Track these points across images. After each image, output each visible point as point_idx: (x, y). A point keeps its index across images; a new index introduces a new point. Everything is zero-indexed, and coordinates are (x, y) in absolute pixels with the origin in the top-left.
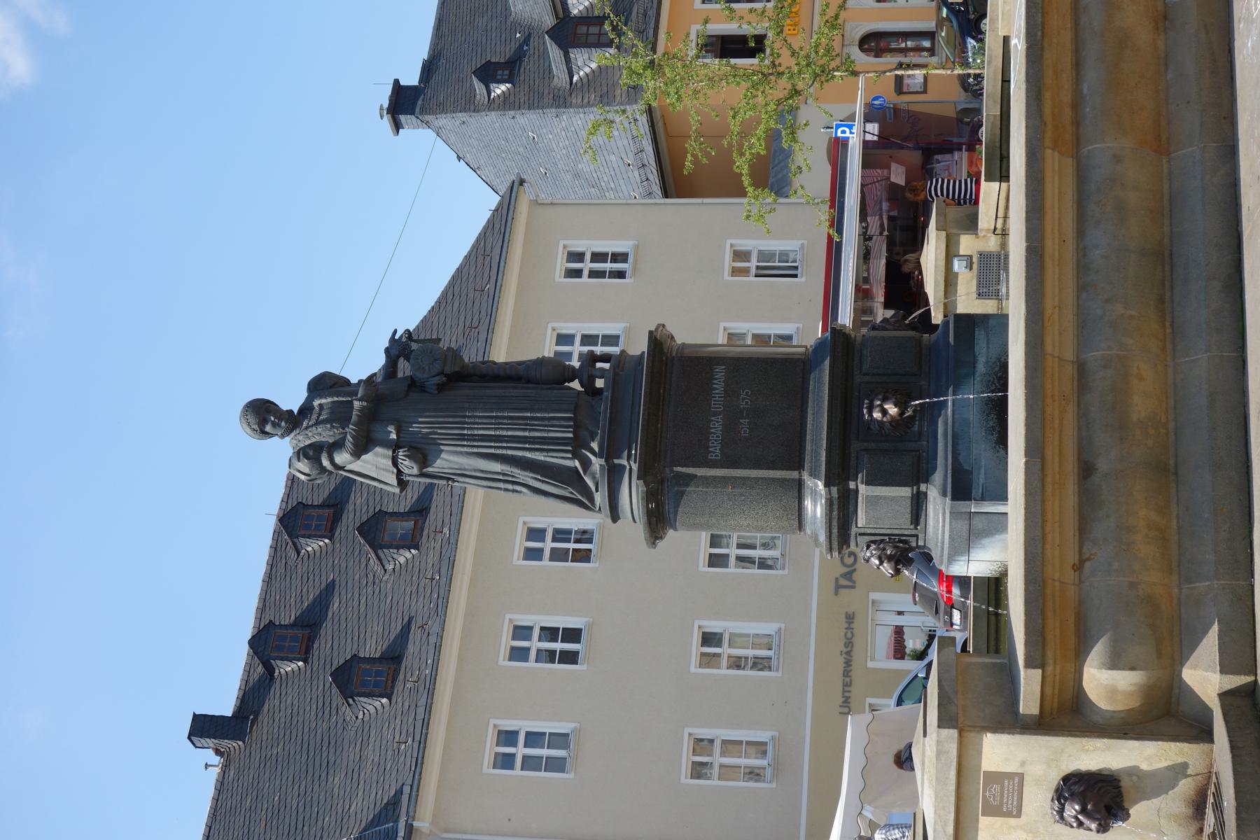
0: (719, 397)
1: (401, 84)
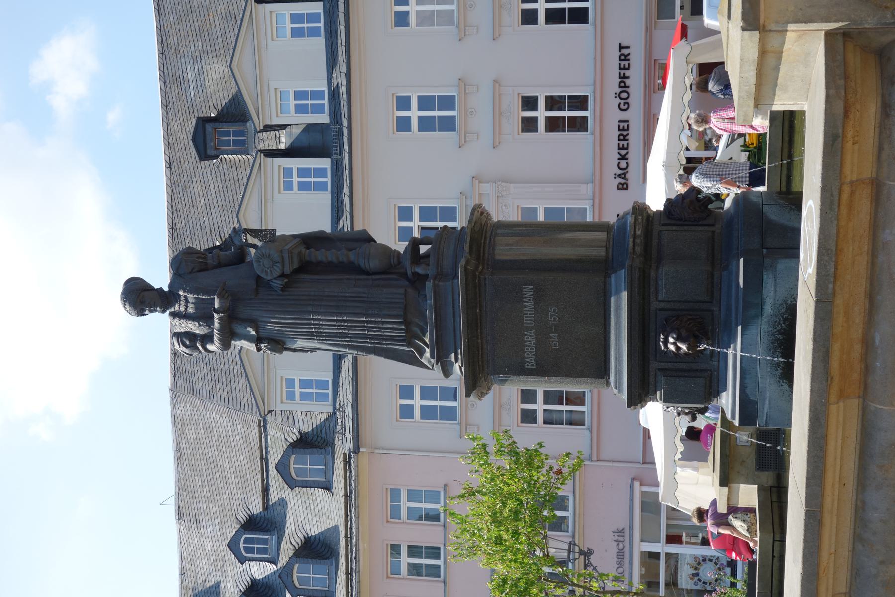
0: (529, 314)
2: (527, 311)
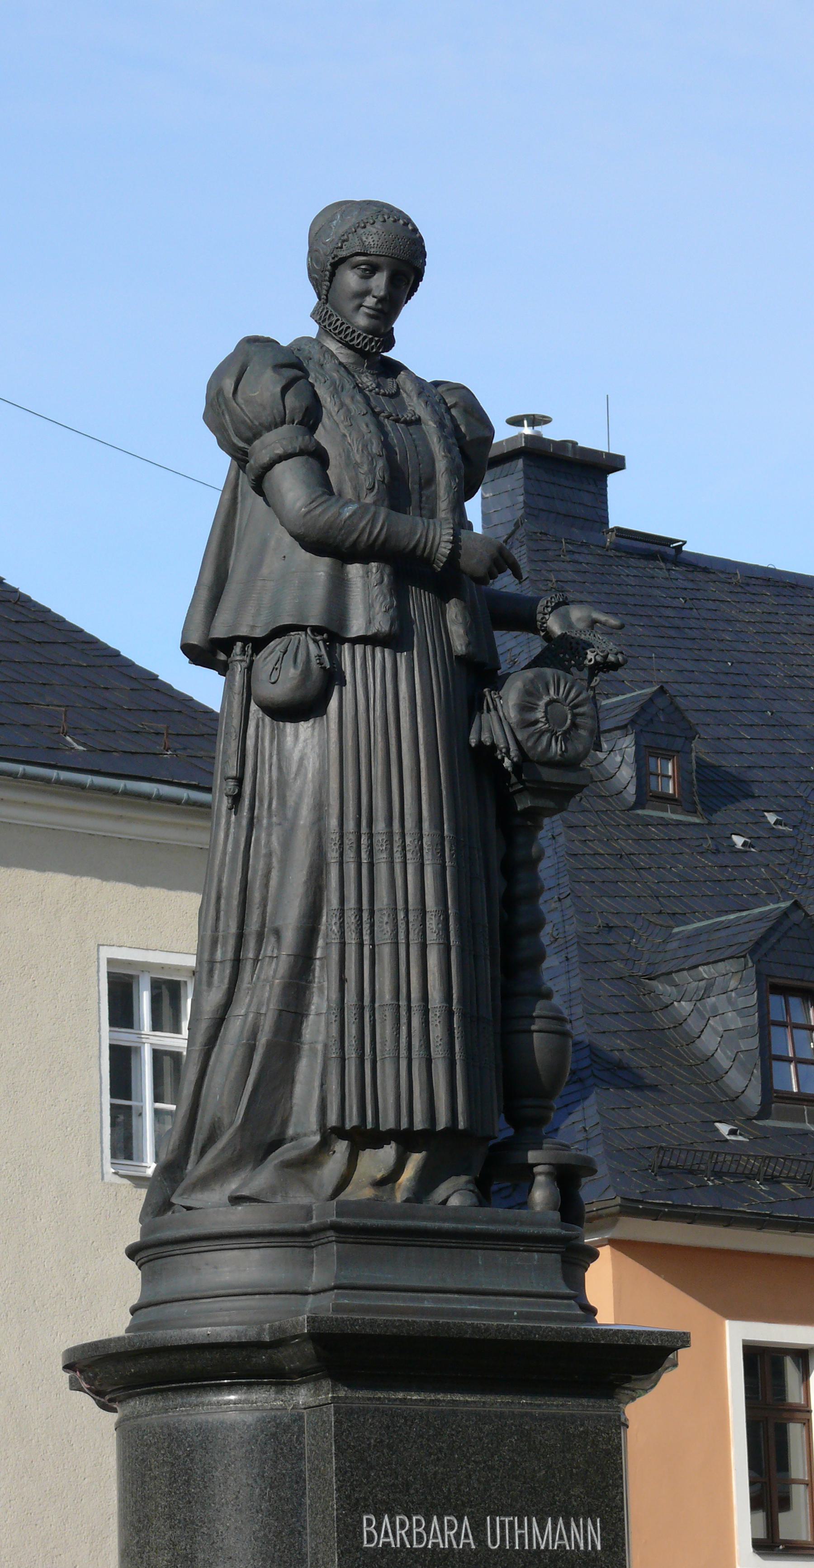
0: (521, 1536)
1: (613, 479)
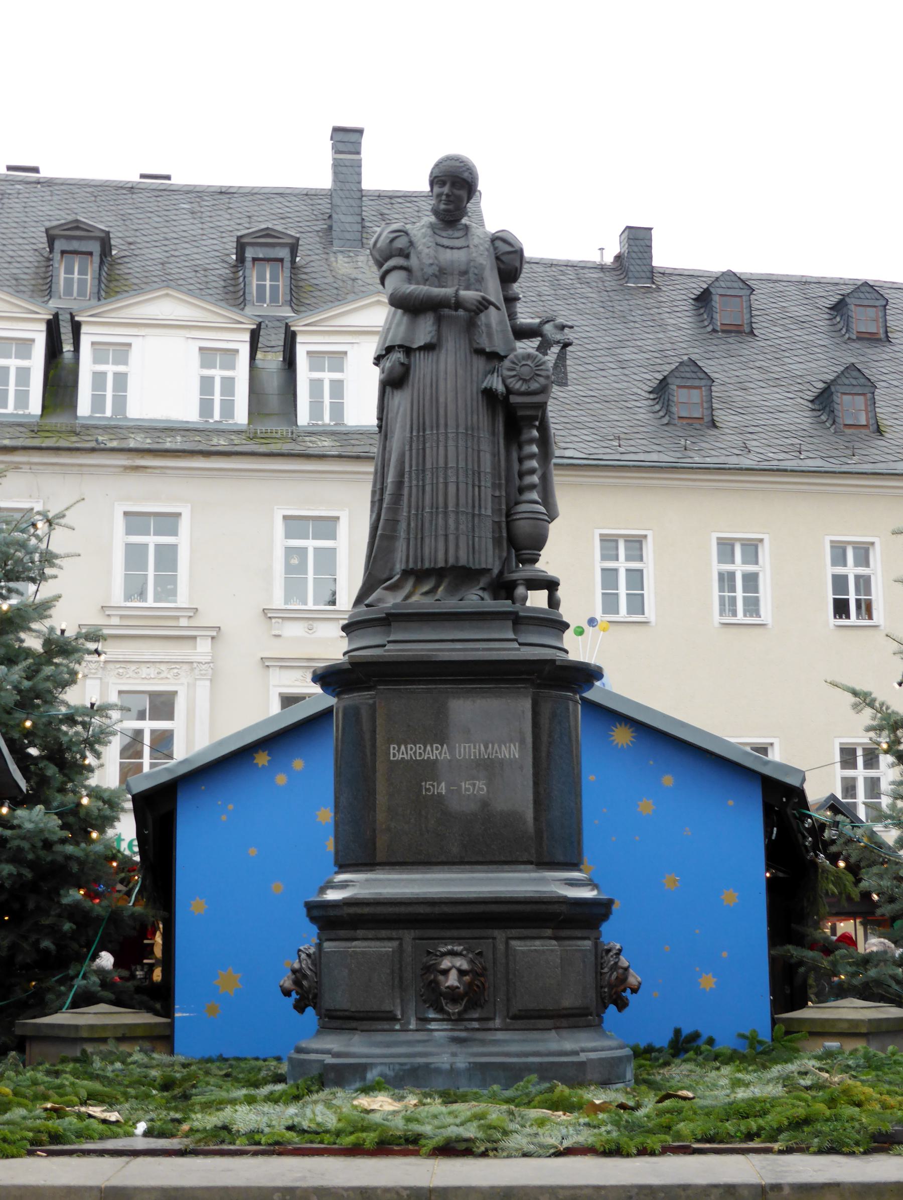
0: (475, 753)
2: (480, 748)
